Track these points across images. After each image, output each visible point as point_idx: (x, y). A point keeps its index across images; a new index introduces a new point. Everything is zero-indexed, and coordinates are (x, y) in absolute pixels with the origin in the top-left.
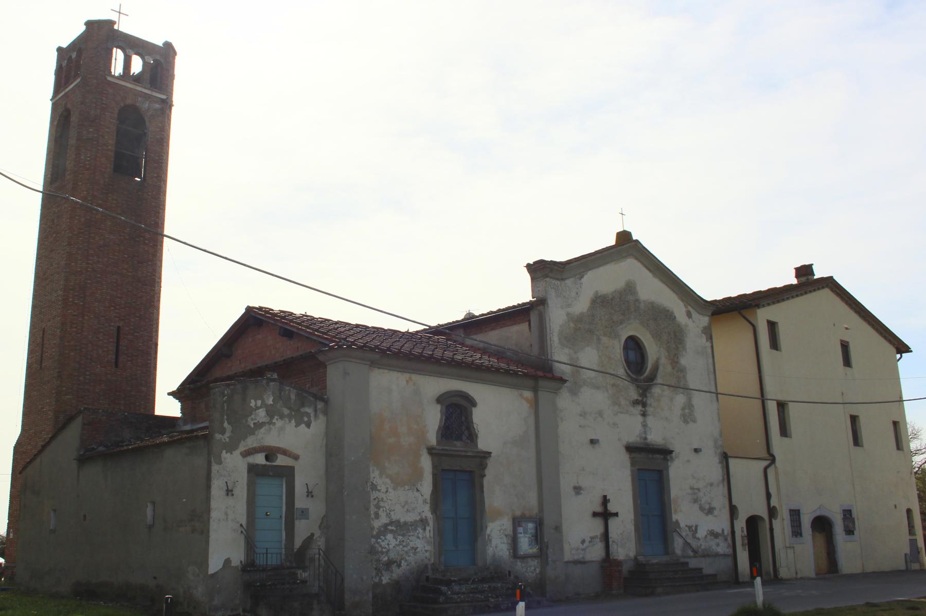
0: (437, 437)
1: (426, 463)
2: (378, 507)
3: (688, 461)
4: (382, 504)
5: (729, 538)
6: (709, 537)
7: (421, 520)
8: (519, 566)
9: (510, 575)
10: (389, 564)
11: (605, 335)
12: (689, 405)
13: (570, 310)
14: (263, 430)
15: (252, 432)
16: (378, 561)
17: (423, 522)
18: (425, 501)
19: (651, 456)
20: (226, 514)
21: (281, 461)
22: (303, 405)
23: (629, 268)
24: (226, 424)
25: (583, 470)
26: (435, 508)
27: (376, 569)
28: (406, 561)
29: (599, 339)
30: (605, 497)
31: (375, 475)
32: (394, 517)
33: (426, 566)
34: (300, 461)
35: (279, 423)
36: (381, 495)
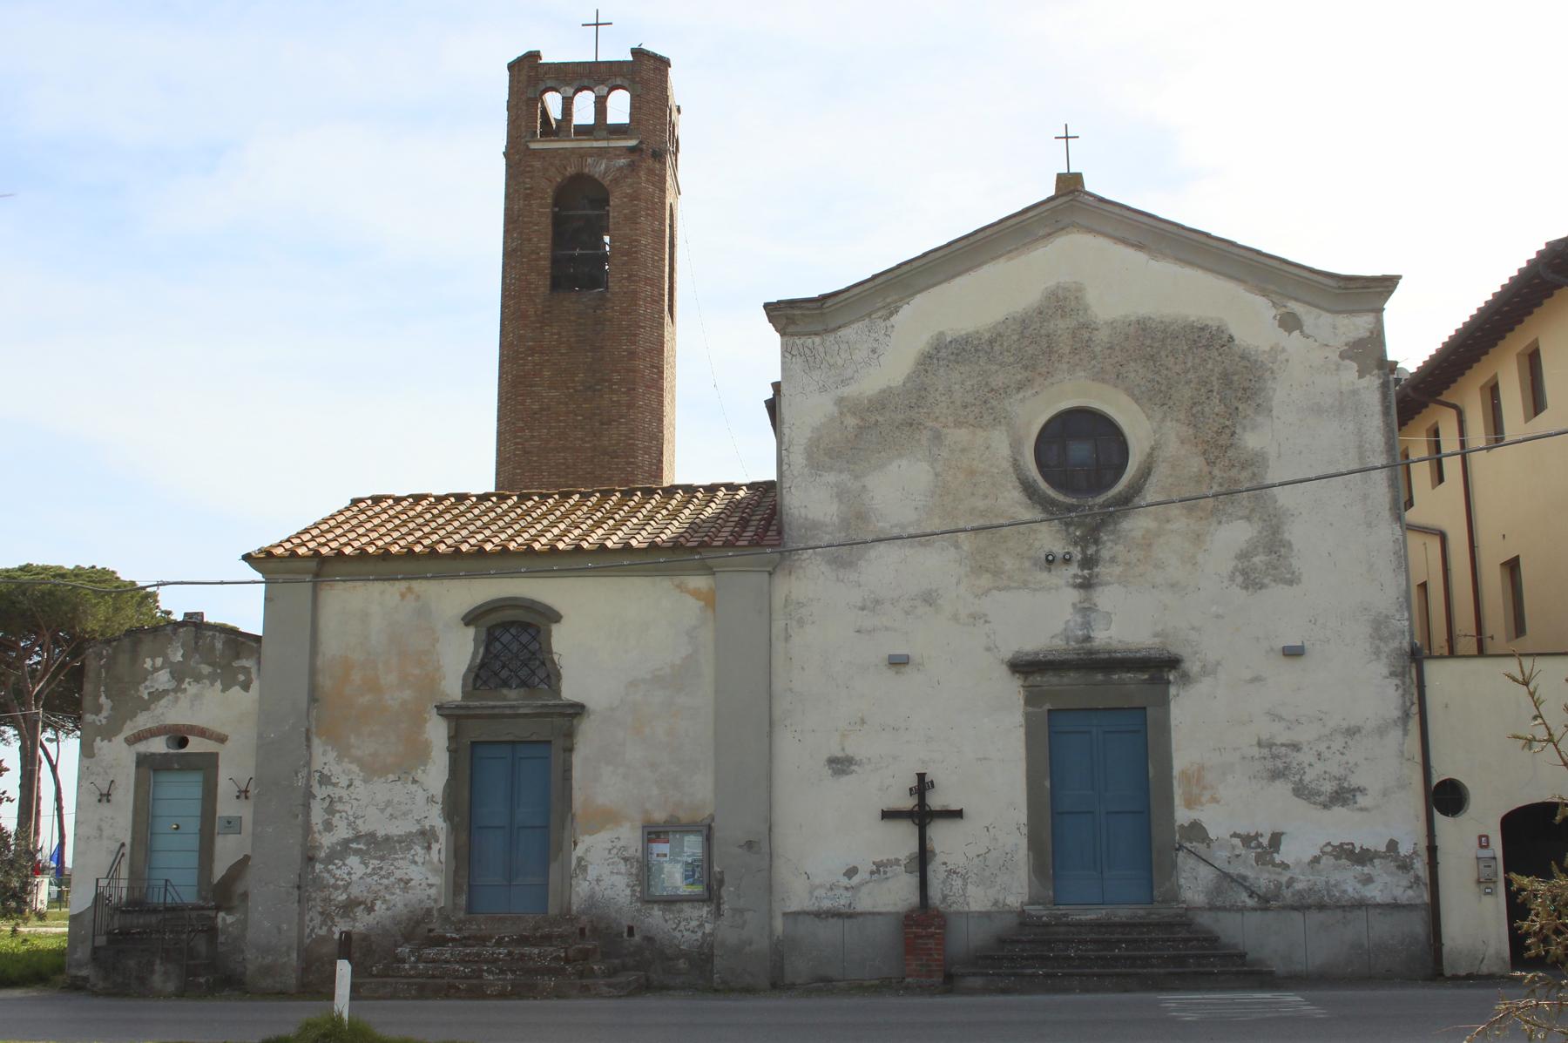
0: (464, 686)
1: (437, 733)
2: (331, 811)
3: (1256, 679)
4: (339, 807)
5: (1421, 867)
6: (1327, 861)
7: (423, 833)
8: (656, 919)
9: (631, 930)
10: (349, 907)
11: (958, 424)
12: (1274, 542)
14: (163, 702)
15: (145, 706)
16: (328, 900)
17: (426, 836)
18: (431, 800)
19: (1100, 677)
20: (100, 829)
21: (195, 745)
22: (238, 657)
24: (103, 699)
25: (863, 722)
26: (450, 813)
27: (322, 914)
28: (385, 901)
29: (937, 437)
30: (921, 776)
31: (324, 757)
32: (363, 828)
33: (429, 911)
34: (228, 744)
35: (191, 688)
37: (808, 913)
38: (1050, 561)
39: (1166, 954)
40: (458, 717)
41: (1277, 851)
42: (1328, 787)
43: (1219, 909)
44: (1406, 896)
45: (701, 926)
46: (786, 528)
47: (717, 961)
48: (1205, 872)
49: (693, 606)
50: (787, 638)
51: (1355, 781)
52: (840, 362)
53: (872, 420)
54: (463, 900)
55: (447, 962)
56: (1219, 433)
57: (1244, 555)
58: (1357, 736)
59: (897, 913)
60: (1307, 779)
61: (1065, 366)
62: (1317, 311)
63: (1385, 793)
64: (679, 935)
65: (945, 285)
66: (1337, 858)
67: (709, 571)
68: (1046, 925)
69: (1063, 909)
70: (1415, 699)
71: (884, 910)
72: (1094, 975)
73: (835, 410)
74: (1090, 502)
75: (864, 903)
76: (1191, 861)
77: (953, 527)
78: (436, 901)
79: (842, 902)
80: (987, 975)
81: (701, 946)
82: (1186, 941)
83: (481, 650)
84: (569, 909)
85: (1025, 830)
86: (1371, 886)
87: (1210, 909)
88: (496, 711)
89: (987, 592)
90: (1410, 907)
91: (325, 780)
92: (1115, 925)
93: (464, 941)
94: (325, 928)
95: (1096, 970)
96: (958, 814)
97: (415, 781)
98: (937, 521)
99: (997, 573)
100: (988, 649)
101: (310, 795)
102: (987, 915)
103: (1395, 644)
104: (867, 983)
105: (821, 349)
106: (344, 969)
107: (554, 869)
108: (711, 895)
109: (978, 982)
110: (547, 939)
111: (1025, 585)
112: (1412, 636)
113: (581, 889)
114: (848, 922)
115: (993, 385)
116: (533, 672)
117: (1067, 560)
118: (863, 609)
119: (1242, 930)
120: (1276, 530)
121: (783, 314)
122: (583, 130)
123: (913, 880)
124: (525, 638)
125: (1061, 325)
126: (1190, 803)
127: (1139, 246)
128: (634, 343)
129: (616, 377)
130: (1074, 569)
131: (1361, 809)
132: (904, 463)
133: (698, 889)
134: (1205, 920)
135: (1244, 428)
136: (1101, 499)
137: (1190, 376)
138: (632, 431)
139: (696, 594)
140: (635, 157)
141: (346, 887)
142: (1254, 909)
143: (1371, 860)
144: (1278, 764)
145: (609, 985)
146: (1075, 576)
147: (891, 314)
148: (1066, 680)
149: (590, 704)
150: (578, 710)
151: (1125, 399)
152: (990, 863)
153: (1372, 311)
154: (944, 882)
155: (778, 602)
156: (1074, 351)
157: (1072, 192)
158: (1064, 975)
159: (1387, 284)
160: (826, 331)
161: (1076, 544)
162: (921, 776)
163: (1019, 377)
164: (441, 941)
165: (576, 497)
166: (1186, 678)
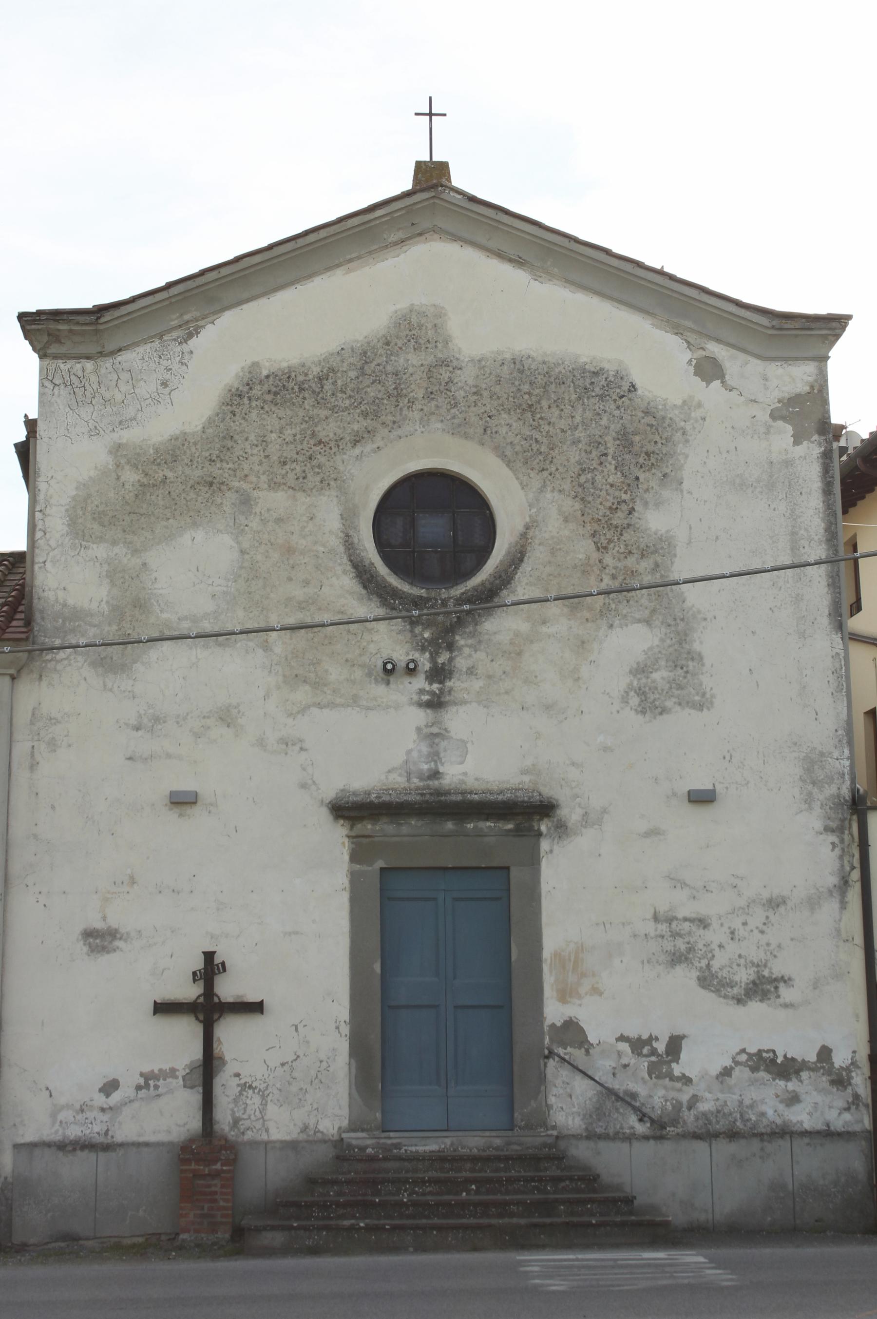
3: (654, 833)
6: (741, 1074)
11: (274, 485)
12: (682, 657)
13: (131, 435)
19: (450, 825)
23: (429, 272)
25: (133, 881)
29: (246, 502)
30: (209, 956)
37: (48, 1145)
38: (389, 671)
39: (528, 1198)
41: (677, 1059)
42: (744, 976)
43: (600, 1137)
44: (841, 1120)
46: (37, 616)
48: (582, 1089)
50: (33, 766)
51: (777, 968)
52: (119, 397)
53: (160, 476)
56: (613, 510)
57: (641, 670)
58: (782, 909)
59: (171, 1144)
60: (716, 965)
61: (416, 415)
62: (742, 356)
63: (816, 985)
65: (263, 301)
66: (754, 1069)
68: (372, 1159)
69: (394, 1138)
71: (152, 1139)
72: (433, 1227)
73: (110, 460)
74: (444, 593)
75: (126, 1130)
76: (565, 1073)
77: (262, 625)
79: (94, 1128)
80: (291, 1228)
82: (556, 1180)
85: (346, 1030)
86: (797, 1108)
87: (588, 1138)
89: (304, 710)
90: (845, 1136)
92: (462, 1159)
95: (436, 1221)
96: (257, 1008)
98: (240, 613)
99: (319, 684)
100: (304, 786)
102: (292, 1146)
103: (832, 790)
104: (128, 1242)
105: (94, 378)
109: (277, 1238)
111: (355, 700)
112: (853, 780)
114: (102, 1156)
115: (322, 435)
117: (411, 671)
118: (137, 728)
119: (630, 1165)
120: (683, 638)
121: (45, 329)
123: (195, 1097)
126: (564, 996)
127: (519, 262)
130: (420, 682)
131: (786, 1006)
132: (200, 535)
134: (581, 1151)
135: (646, 504)
136: (458, 591)
137: (580, 434)
142: (646, 1138)
143: (797, 1072)
144: (679, 944)
146: (421, 691)
147: (190, 336)
148: (405, 829)
151: (494, 462)
152: (297, 1079)
153: (813, 359)
154: (235, 1101)
155: (22, 716)
156: (430, 395)
157: (434, 187)
158: (394, 1228)
159: (833, 325)
160: (101, 354)
161: (423, 649)
162: (209, 956)
163: (356, 427)
166: (562, 829)
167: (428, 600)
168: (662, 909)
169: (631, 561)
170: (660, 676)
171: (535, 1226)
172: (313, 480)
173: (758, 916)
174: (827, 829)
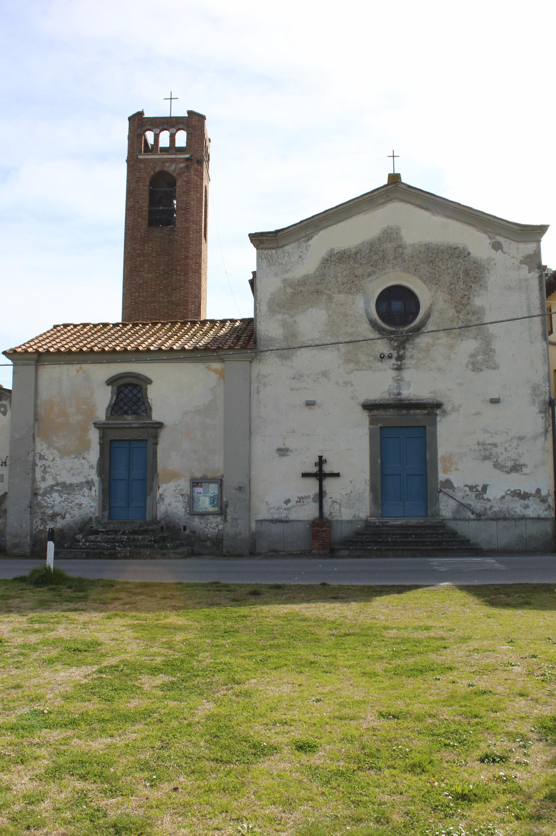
0: (106, 414)
1: (94, 436)
2: (45, 472)
3: (477, 414)
4: (48, 470)
6: (508, 498)
7: (88, 482)
8: (197, 522)
9: (185, 528)
10: (54, 516)
11: (340, 292)
12: (488, 351)
13: (289, 276)
16: (44, 513)
17: (89, 484)
18: (91, 467)
19: (404, 412)
23: (395, 213)
26: (100, 473)
27: (41, 519)
28: (70, 514)
29: (330, 298)
30: (320, 457)
31: (41, 447)
32: (60, 480)
33: (91, 519)
36: (47, 463)
37: (267, 520)
38: (382, 357)
39: (433, 540)
40: (104, 428)
41: (485, 493)
42: (510, 464)
43: (458, 520)
45: (217, 526)
46: (258, 340)
47: (224, 542)
49: (214, 377)
50: (258, 392)
51: (522, 461)
52: (284, 262)
53: (300, 289)
54: (106, 513)
55: (100, 542)
57: (473, 356)
58: (524, 441)
59: (309, 520)
60: (500, 460)
61: (390, 265)
62: (509, 241)
63: (535, 467)
64: (207, 530)
65: (335, 226)
66: (513, 496)
67: (222, 360)
68: (378, 526)
69: (386, 520)
70: (551, 424)
71: (302, 519)
72: (399, 550)
73: (282, 284)
74: (401, 329)
75: (293, 516)
77: (337, 341)
78: (94, 514)
80: (350, 549)
81: (217, 535)
83: (115, 397)
84: (156, 518)
85: (368, 483)
86: (528, 510)
87: (453, 520)
88: (122, 426)
89: (352, 372)
90: (545, 519)
91: (42, 457)
92: (409, 526)
93: (107, 533)
94: (43, 526)
95: (400, 547)
96: (337, 475)
97: (84, 458)
98: (329, 338)
99: (357, 362)
100: (352, 398)
101: (35, 464)
102: (350, 522)
103: (542, 398)
104: (295, 553)
105: (275, 256)
106: (51, 545)
107: (149, 499)
108: (222, 512)
109: (346, 552)
110: (146, 532)
111: (370, 368)
112: (550, 395)
113: (162, 509)
114: (285, 524)
115: (357, 274)
116: (139, 408)
117: (390, 357)
118: (294, 379)
119: (469, 529)
120: (488, 344)
121: (259, 240)
122: (164, 150)
123: (317, 505)
124: (135, 392)
125: (389, 246)
127: (427, 209)
128: (188, 252)
129: (179, 268)
130: (393, 361)
131: (525, 474)
132: (314, 310)
133: (216, 509)
134: (451, 525)
135: (474, 296)
136: (406, 328)
137: (450, 271)
138: (187, 294)
139: (215, 371)
140: (189, 163)
141: (53, 507)
142: (474, 520)
143: (528, 497)
144: (486, 453)
145: (174, 553)
146: (394, 364)
147: (309, 240)
148: (388, 413)
149: (166, 423)
150: (160, 425)
151: (419, 282)
152: (352, 499)
153: (535, 241)
155: (254, 375)
156: (395, 258)
157: (395, 183)
158: (386, 550)
159: (542, 229)
160: (278, 247)
161: (394, 349)
162: (320, 457)
163: (369, 270)
164: (96, 532)
165: (160, 325)
166: (444, 412)
167: (396, 332)
168: (481, 440)
169: (469, 317)
170: (480, 358)
171: (435, 549)
172: (354, 290)
173: (515, 443)
174: (541, 412)
